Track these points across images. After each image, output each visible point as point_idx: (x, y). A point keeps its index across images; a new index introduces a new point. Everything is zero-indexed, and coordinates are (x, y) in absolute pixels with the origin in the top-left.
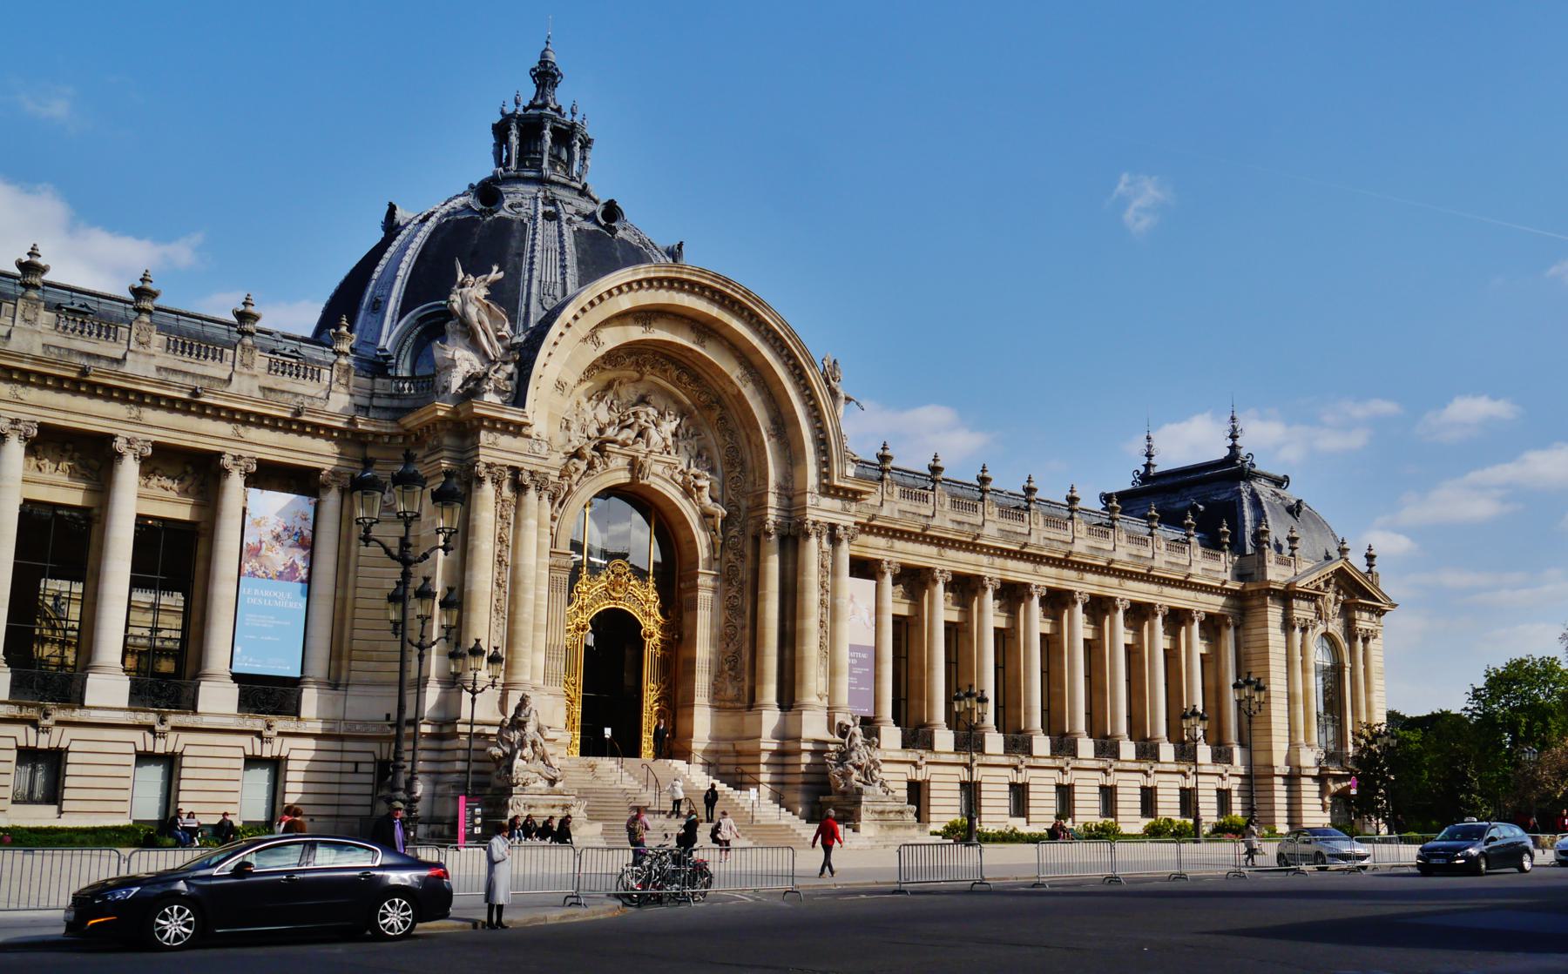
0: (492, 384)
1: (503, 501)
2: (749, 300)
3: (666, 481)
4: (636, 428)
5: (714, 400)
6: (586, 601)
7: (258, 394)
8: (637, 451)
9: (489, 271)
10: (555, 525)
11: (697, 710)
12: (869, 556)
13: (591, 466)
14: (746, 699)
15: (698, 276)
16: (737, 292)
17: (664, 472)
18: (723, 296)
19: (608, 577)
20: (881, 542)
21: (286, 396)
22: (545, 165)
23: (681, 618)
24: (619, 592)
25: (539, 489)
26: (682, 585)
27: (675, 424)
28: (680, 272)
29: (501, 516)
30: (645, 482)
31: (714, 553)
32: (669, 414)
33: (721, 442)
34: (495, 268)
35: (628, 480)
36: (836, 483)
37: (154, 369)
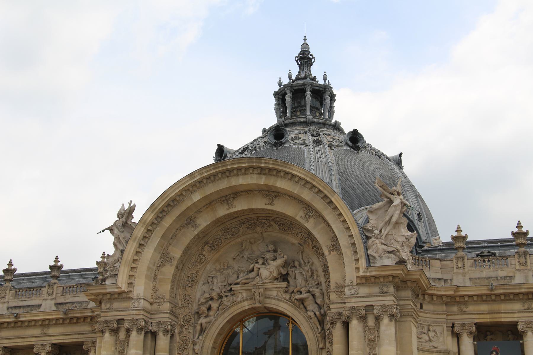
0: (108, 274)
2: (279, 165)
3: (279, 300)
5: (305, 236)
7: (54, 308)
8: (254, 285)
12: (503, 320)
15: (238, 163)
16: (269, 163)
17: (277, 295)
18: (262, 169)
20: (517, 306)
21: (68, 305)
22: (308, 113)
25: (140, 330)
27: (279, 262)
28: (225, 166)
30: (258, 305)
32: (280, 255)
35: (251, 306)
36: (361, 273)
37: (6, 309)
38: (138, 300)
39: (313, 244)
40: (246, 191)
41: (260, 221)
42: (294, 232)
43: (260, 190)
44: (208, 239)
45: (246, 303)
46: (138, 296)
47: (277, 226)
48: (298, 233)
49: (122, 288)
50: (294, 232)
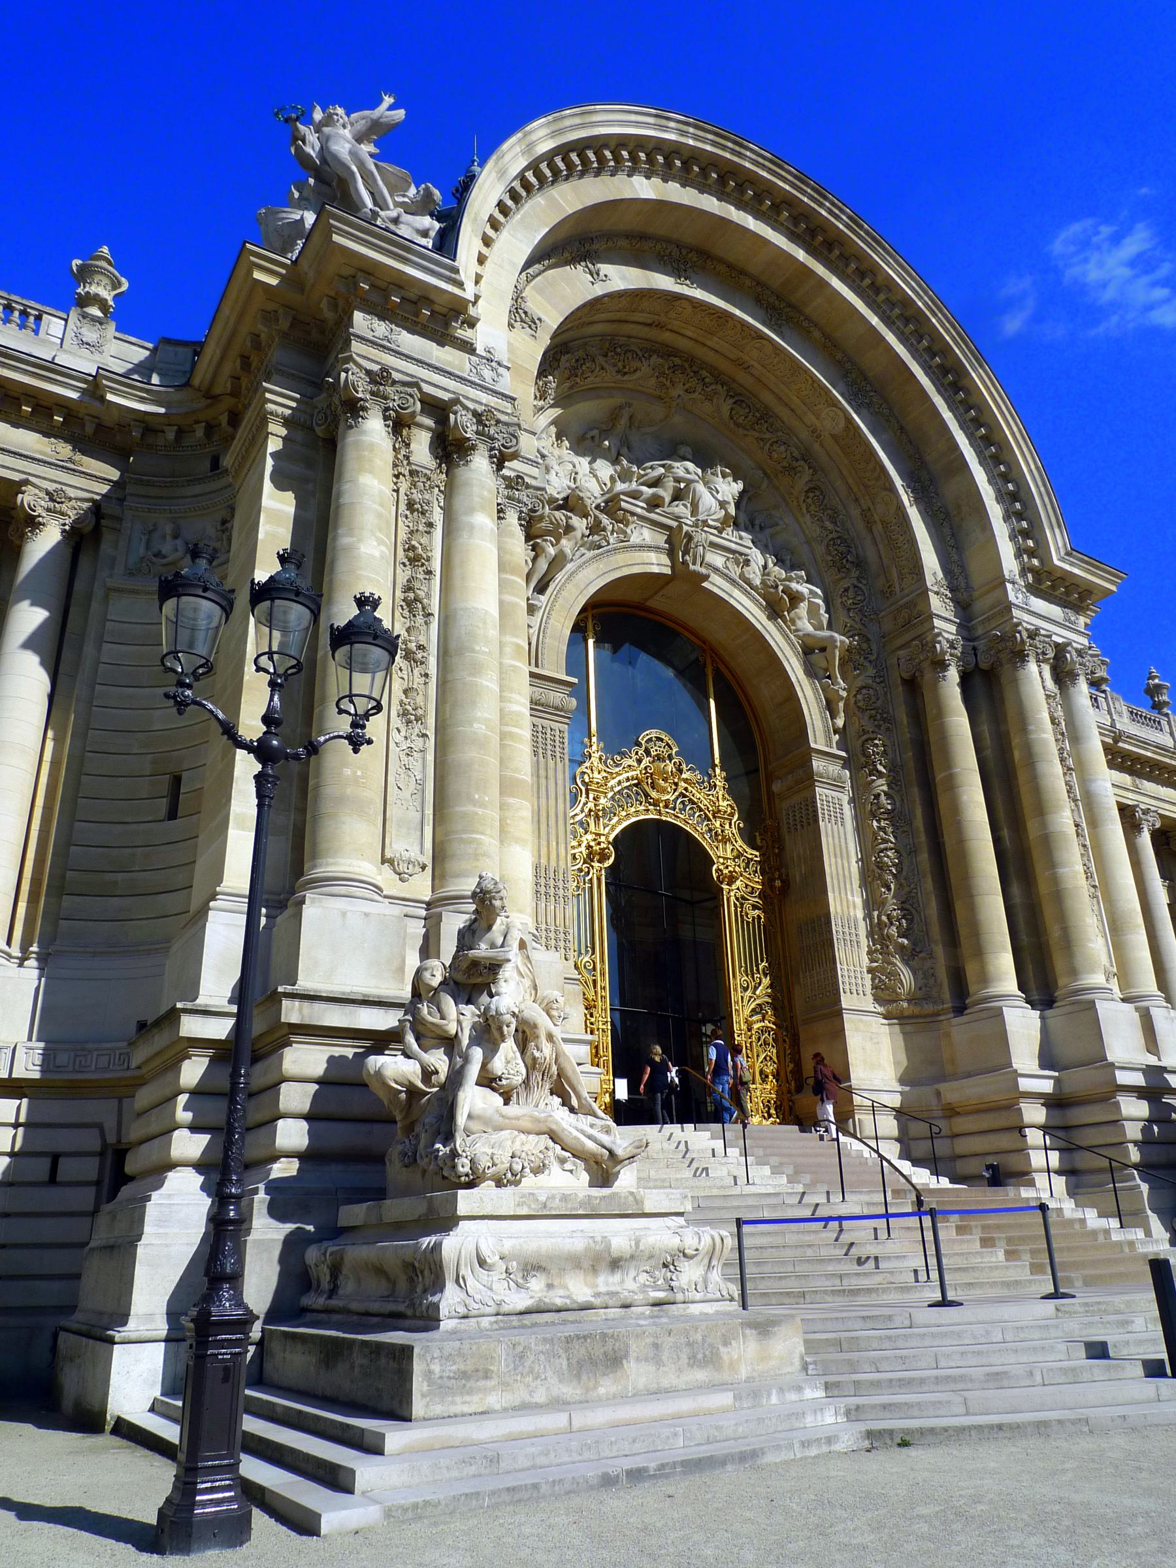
1: (412, 473)
3: (732, 582)
4: (670, 484)
5: (796, 454)
6: (603, 801)
9: (375, 103)
10: (536, 620)
11: (850, 1023)
13: (596, 528)
14: (946, 994)
15: (769, 171)
19: (639, 761)
23: (782, 849)
24: (664, 791)
26: (776, 787)
28: (739, 155)
29: (410, 505)
31: (833, 717)
33: (814, 530)
34: (388, 100)
38: (494, 364)
39: (810, 481)
40: (730, 266)
41: (694, 368)
42: (767, 436)
43: (758, 283)
44: (571, 344)
45: (653, 557)
46: (489, 352)
47: (733, 401)
48: (777, 442)
49: (464, 290)
50: (767, 436)
